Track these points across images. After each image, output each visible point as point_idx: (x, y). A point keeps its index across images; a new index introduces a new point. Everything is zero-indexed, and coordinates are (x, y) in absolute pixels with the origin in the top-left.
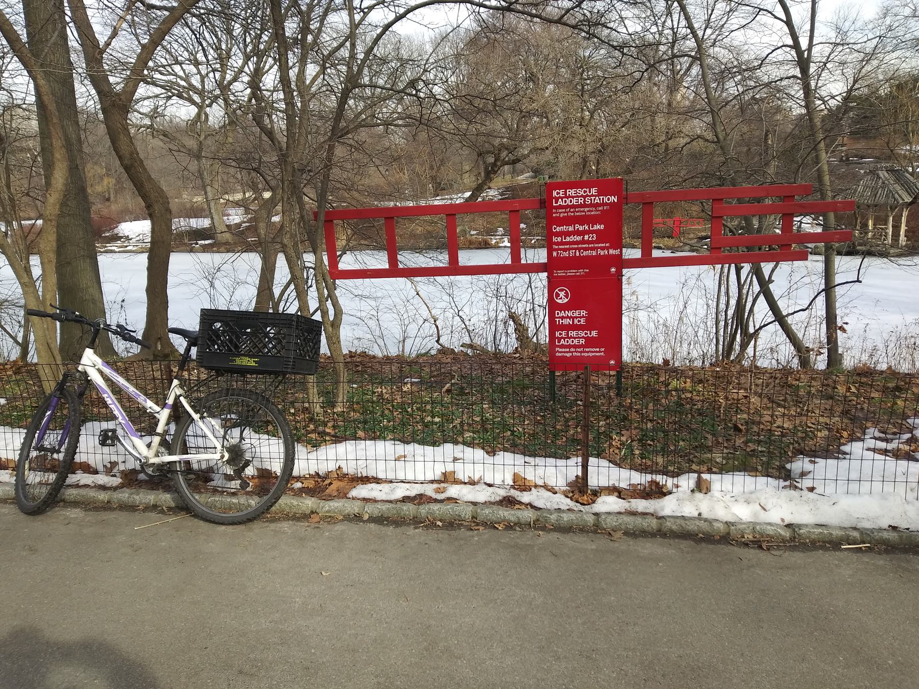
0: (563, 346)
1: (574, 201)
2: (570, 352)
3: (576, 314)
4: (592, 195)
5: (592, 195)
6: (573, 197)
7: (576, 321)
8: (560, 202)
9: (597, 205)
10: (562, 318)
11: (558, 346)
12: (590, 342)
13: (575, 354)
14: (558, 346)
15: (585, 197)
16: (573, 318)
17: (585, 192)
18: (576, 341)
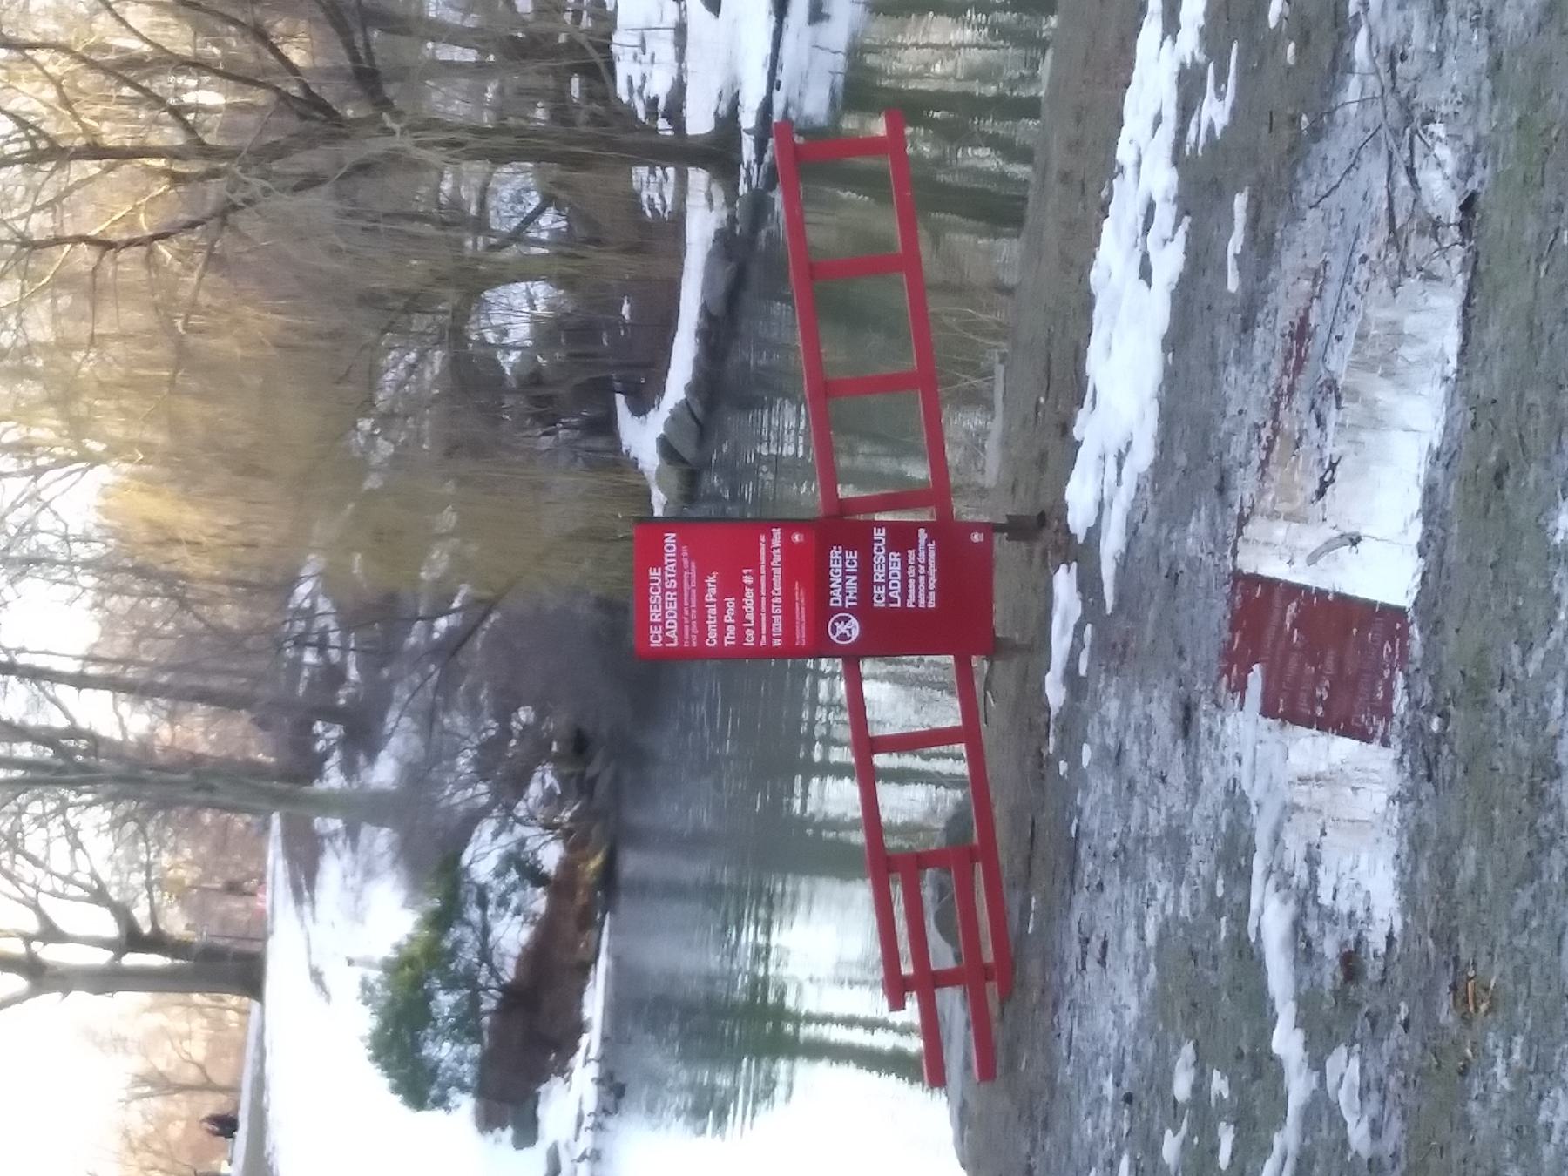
1: (672, 608)
4: (663, 576)
5: (663, 576)
6: (664, 610)
8: (672, 634)
9: (680, 568)
15: (664, 590)
17: (655, 590)
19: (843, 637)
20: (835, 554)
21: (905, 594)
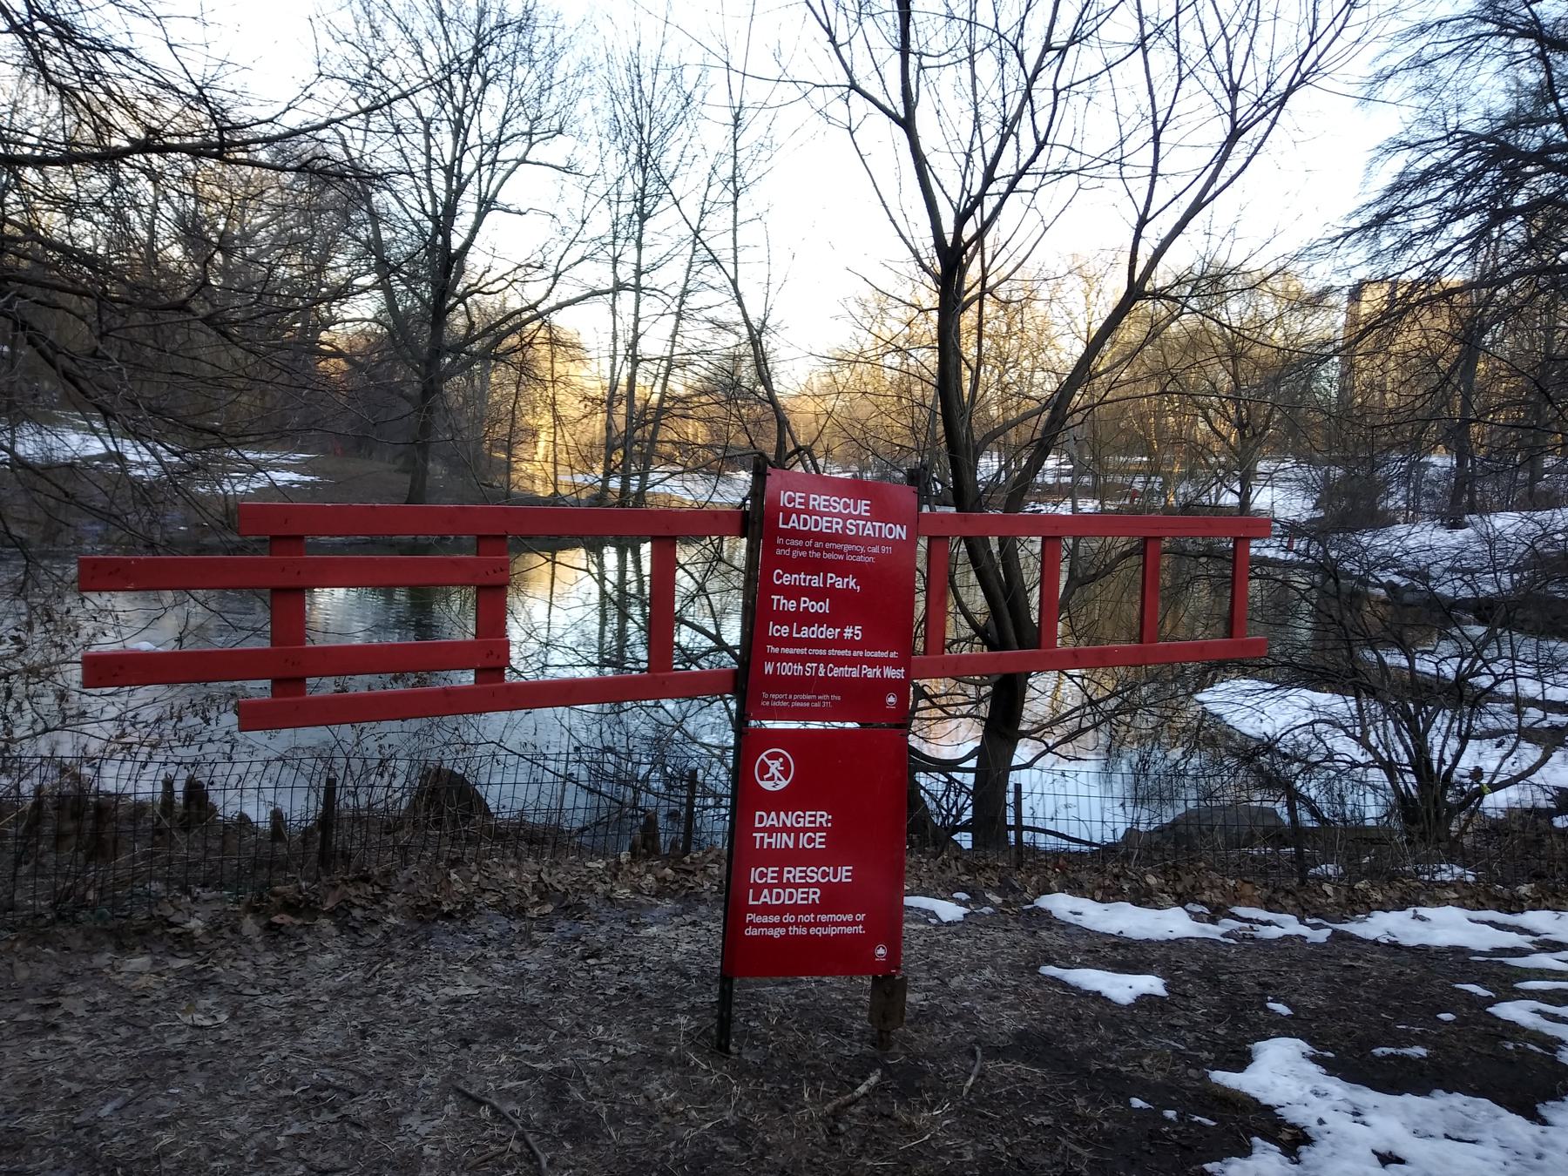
0: (766, 909)
2: (781, 924)
3: (806, 819)
4: (860, 517)
5: (860, 517)
7: (803, 840)
10: (771, 830)
11: (754, 909)
12: (833, 898)
13: (793, 930)
14: (754, 909)
16: (797, 831)
18: (798, 897)
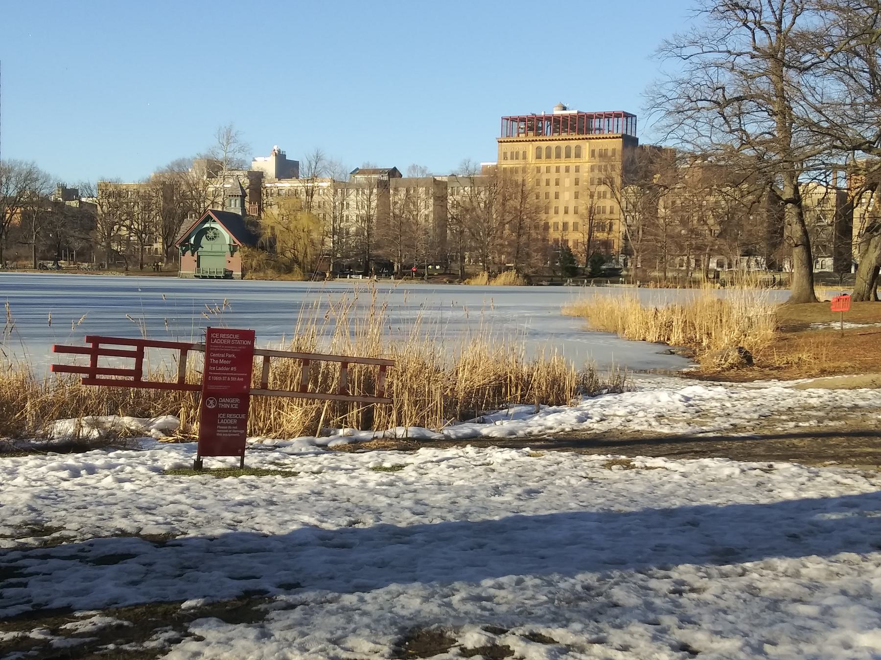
9: (238, 345)
19: (208, 402)
20: (237, 400)
21: (222, 425)
